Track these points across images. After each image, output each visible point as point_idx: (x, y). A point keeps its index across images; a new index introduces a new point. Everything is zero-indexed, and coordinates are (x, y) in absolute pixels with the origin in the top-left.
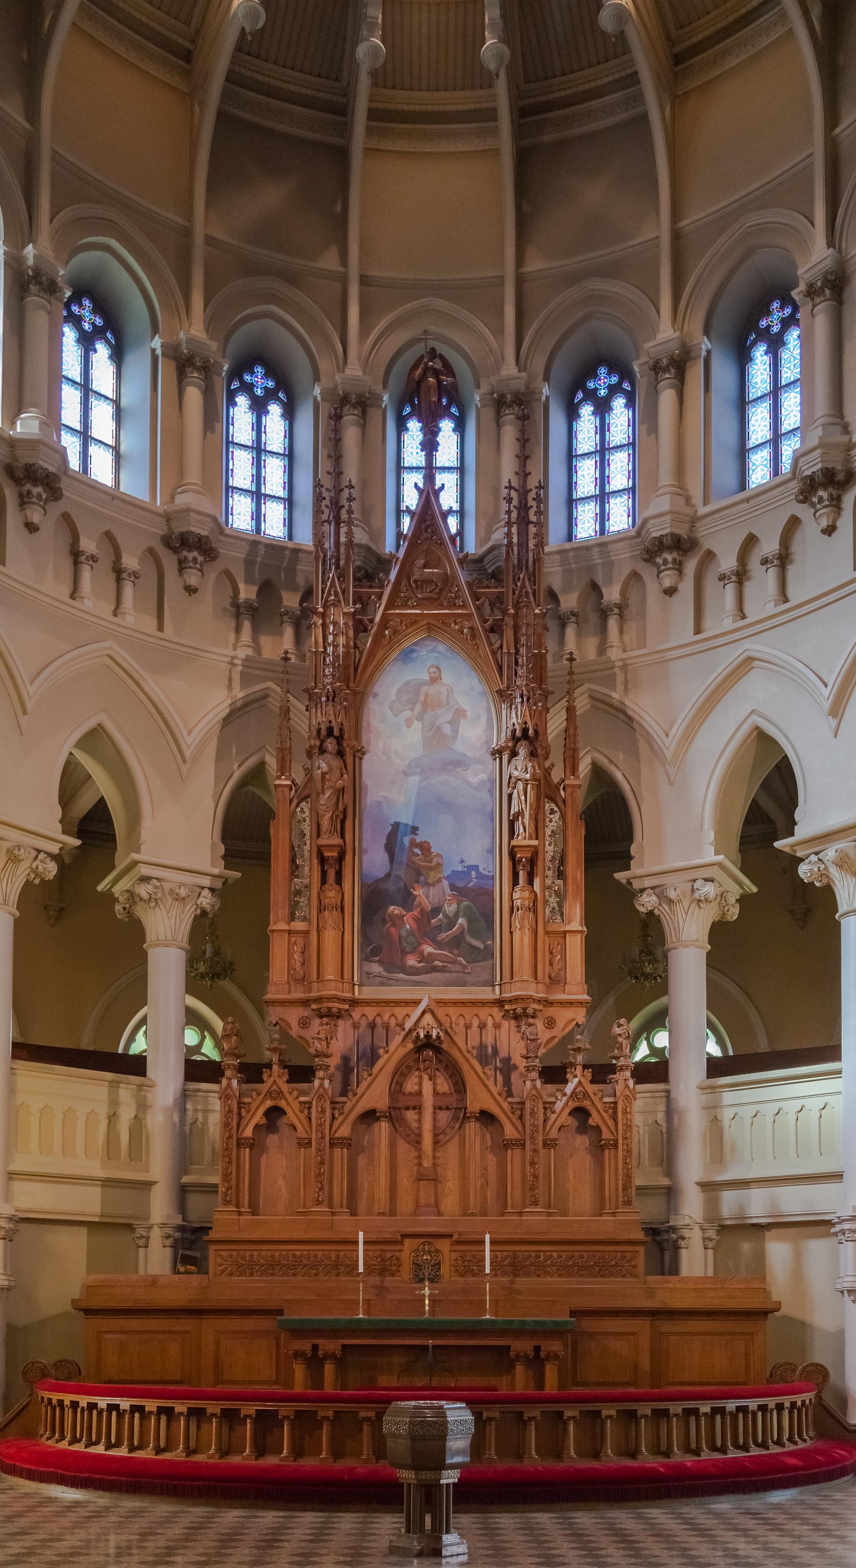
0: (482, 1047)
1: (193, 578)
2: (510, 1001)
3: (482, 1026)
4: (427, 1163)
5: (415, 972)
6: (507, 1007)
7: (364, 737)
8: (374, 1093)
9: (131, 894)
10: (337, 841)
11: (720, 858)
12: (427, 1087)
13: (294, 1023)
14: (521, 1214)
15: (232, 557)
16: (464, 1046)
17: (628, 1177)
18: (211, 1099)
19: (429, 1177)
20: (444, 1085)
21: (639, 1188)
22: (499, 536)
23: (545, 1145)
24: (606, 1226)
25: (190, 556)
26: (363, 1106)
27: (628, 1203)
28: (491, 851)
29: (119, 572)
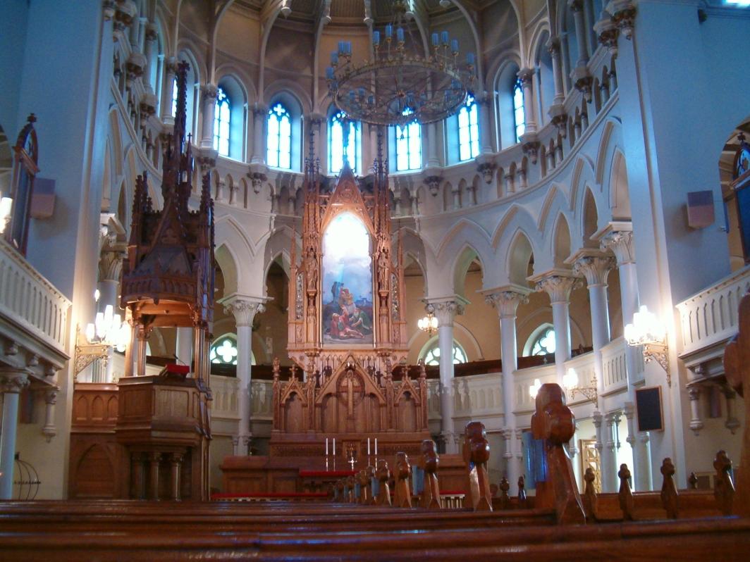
0: (369, 367)
1: (258, 188)
2: (381, 350)
3: (369, 359)
4: (351, 413)
5: (344, 338)
6: (379, 352)
7: (323, 250)
9: (232, 306)
10: (315, 290)
11: (456, 295)
12: (349, 383)
13: (298, 359)
14: (386, 432)
15: (272, 179)
17: (425, 417)
19: (351, 418)
20: (356, 383)
21: (429, 420)
22: (371, 172)
23: (395, 406)
24: (417, 436)
25: (257, 181)
26: (326, 392)
27: (426, 427)
28: (371, 293)
29: (232, 188)
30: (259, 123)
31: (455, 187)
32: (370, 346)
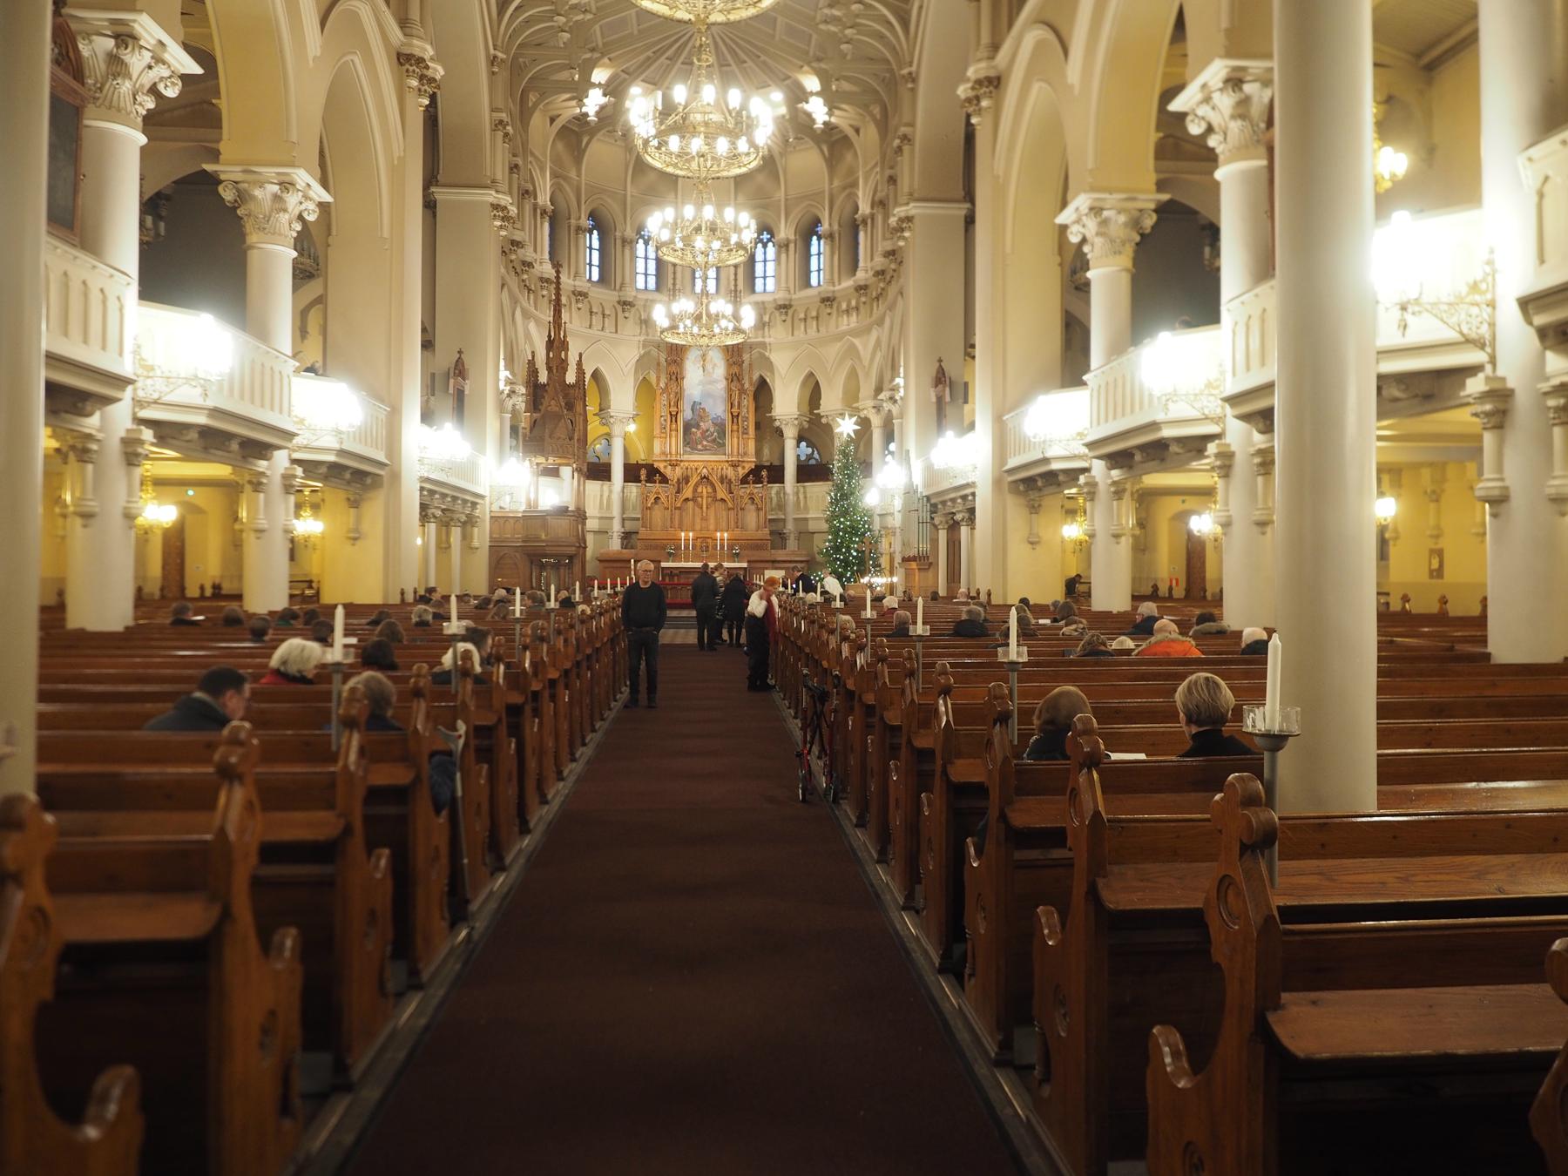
12: (704, 490)
16: (715, 479)
30: (627, 252)
32: (723, 458)
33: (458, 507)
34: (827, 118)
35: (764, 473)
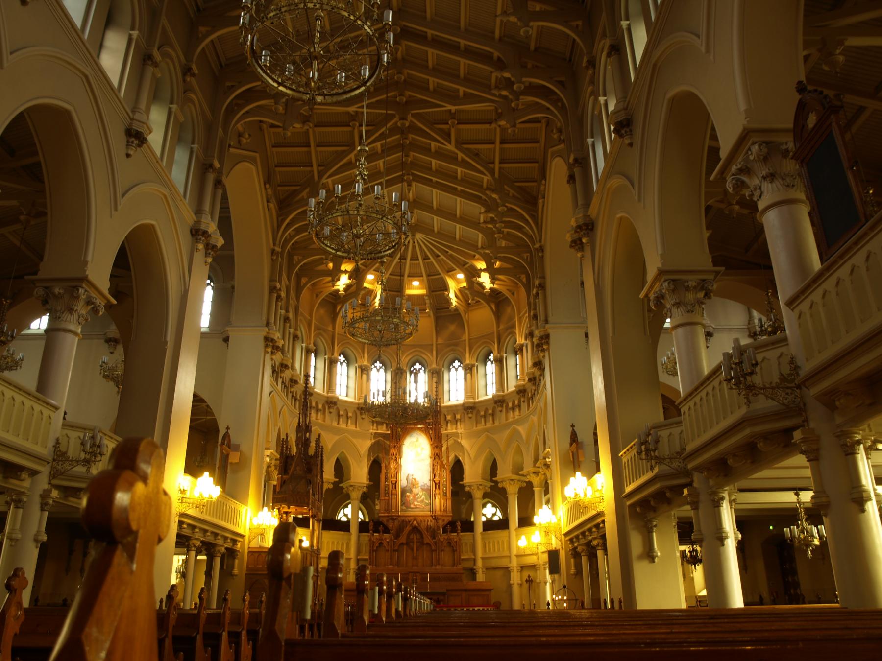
8: (403, 539)
12: (415, 537)
18: (365, 536)
20: (419, 536)
26: (401, 541)
31: (482, 413)
33: (220, 541)
34: (492, 286)
35: (459, 524)
